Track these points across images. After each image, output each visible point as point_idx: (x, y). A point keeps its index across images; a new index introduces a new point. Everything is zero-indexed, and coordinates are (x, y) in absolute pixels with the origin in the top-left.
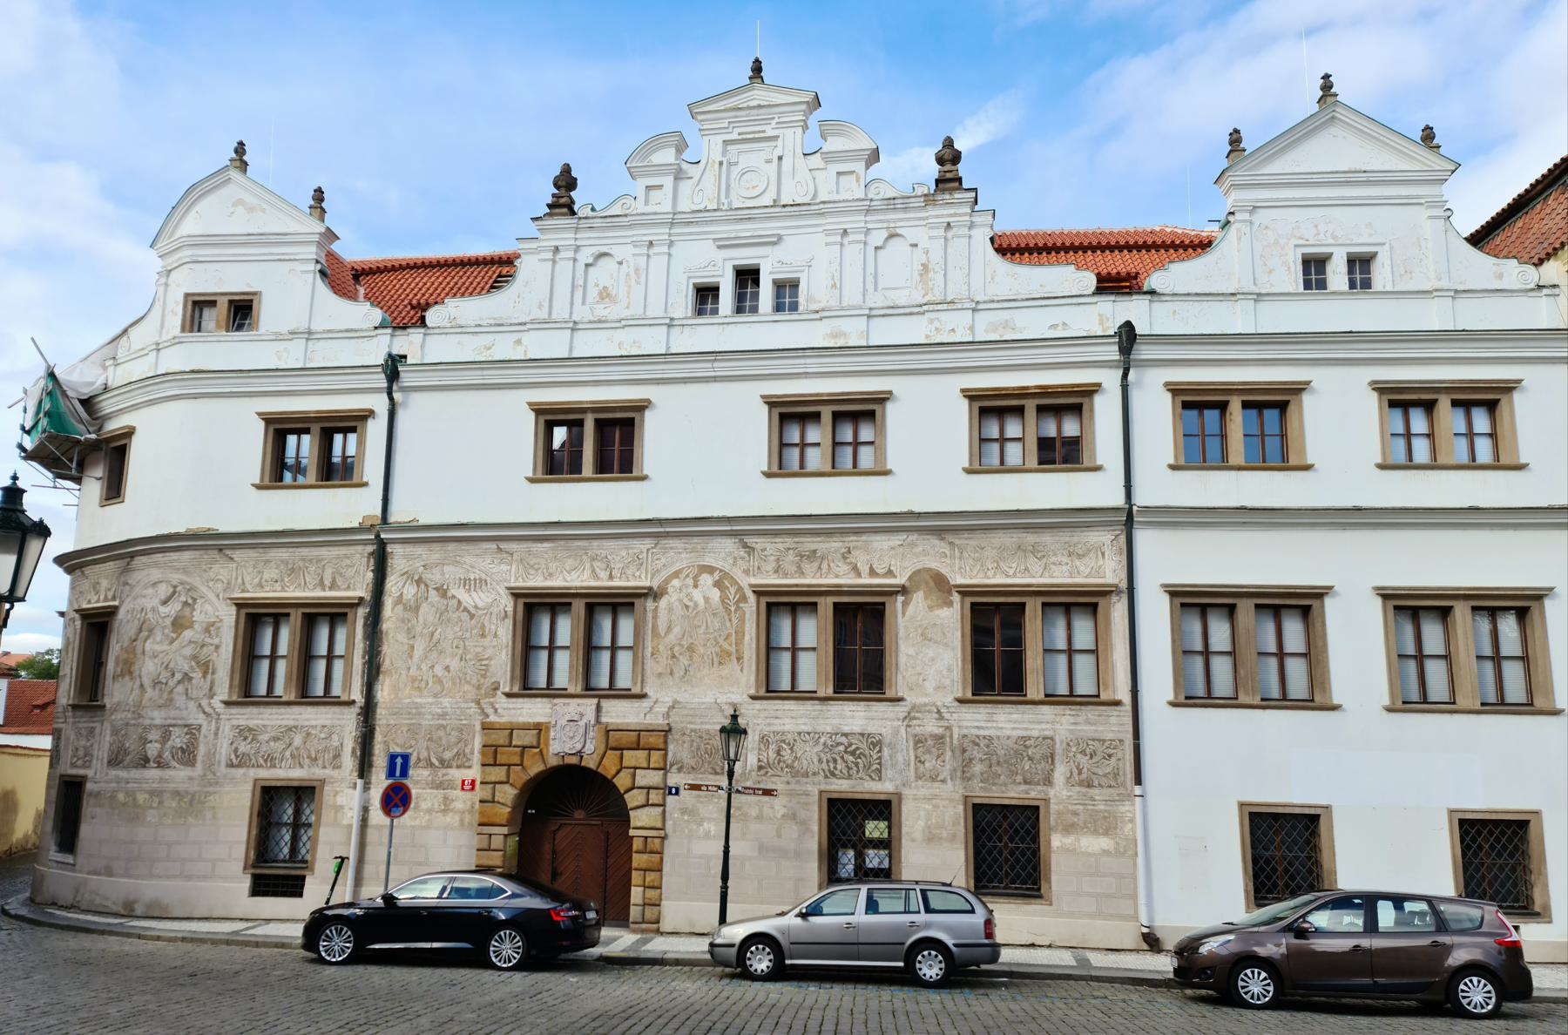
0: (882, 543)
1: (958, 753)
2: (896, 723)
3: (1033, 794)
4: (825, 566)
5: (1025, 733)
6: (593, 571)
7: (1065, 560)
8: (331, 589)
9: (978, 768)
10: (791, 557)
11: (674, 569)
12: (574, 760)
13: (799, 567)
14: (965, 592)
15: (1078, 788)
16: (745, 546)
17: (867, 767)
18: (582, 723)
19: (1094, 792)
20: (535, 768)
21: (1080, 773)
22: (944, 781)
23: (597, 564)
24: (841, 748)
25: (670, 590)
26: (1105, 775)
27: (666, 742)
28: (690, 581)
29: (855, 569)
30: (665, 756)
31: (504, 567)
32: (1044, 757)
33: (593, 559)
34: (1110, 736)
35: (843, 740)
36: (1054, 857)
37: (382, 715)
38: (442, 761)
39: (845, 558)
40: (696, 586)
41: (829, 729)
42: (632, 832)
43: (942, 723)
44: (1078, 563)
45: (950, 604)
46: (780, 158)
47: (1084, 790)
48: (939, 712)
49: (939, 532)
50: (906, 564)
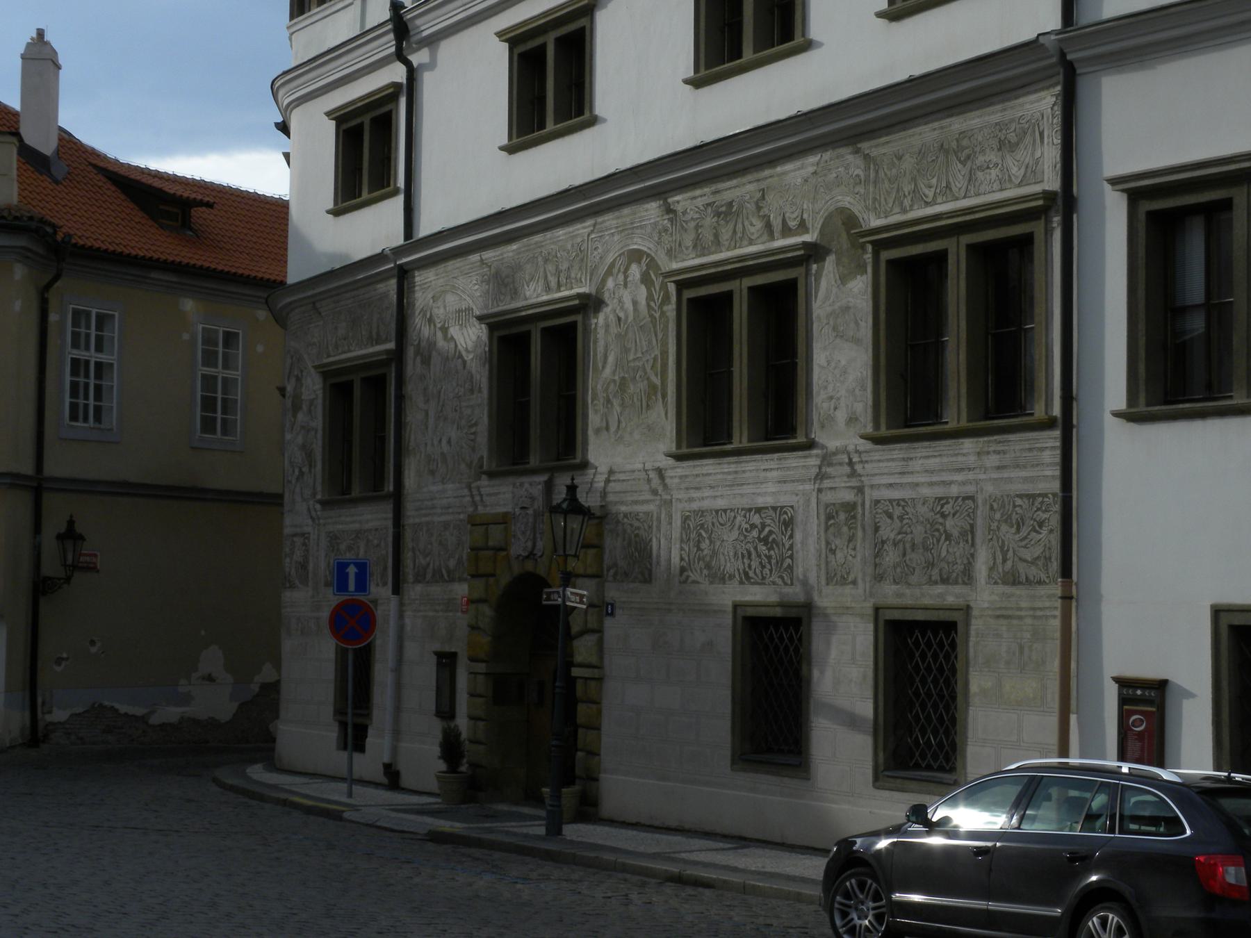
0: (796, 172)
1: (870, 531)
2: (808, 487)
3: (950, 600)
5: (939, 491)
7: (993, 157)
8: (377, 343)
9: (891, 557)
10: (709, 221)
11: (609, 259)
12: (529, 566)
13: (716, 236)
14: (882, 242)
15: (1001, 588)
17: (780, 562)
18: (530, 512)
19: (1018, 591)
20: (505, 580)
21: (1005, 560)
22: (854, 582)
24: (755, 533)
25: (606, 296)
26: (1034, 562)
27: (600, 535)
28: (621, 277)
29: (768, 226)
30: (600, 558)
32: (963, 534)
33: (546, 261)
34: (1041, 487)
35: (756, 519)
36: (972, 711)
37: (412, 516)
38: (449, 572)
39: (759, 208)
40: (625, 285)
41: (745, 502)
42: (575, 672)
43: (854, 482)
44: (1009, 161)
45: (861, 269)
47: (1008, 589)
48: (851, 463)
49: (853, 138)
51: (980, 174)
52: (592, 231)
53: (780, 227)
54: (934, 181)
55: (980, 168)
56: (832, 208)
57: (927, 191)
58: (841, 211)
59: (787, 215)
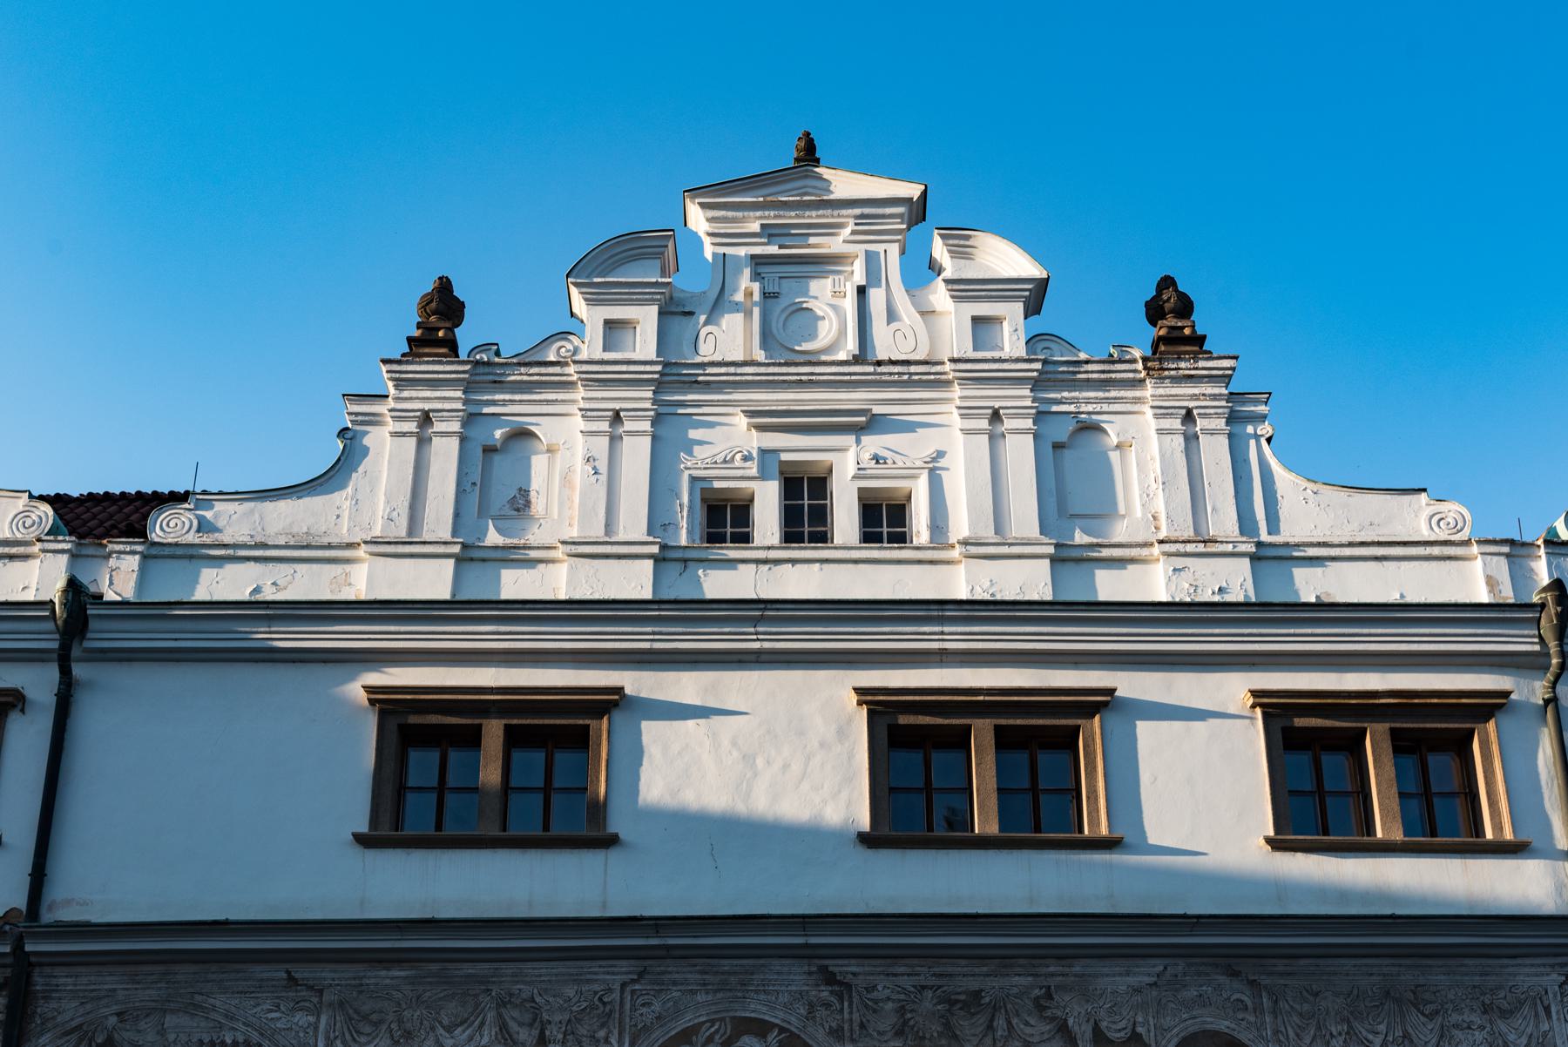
0: (1118, 981)
4: (1000, 1023)
6: (503, 1027)
7: (1476, 1019)
10: (928, 1002)
16: (830, 979)
23: (511, 1014)
31: (302, 1019)
33: (502, 1003)
39: (1040, 1007)
44: (1502, 1026)
46: (861, 291)
49: (1229, 961)
50: (1168, 1021)
51: (1455, 1032)
52: (633, 981)
53: (1089, 1034)
54: (1382, 1028)
55: (1457, 1026)
56: (1192, 1030)
57: (1371, 1037)
58: (1216, 1034)
59: (1104, 1025)
